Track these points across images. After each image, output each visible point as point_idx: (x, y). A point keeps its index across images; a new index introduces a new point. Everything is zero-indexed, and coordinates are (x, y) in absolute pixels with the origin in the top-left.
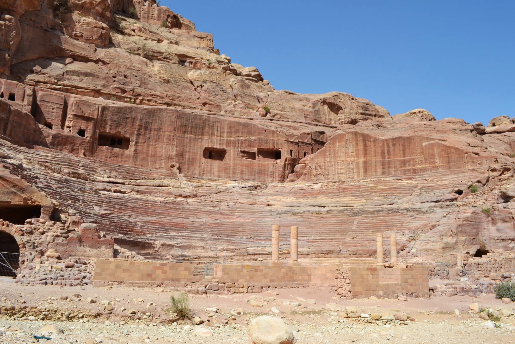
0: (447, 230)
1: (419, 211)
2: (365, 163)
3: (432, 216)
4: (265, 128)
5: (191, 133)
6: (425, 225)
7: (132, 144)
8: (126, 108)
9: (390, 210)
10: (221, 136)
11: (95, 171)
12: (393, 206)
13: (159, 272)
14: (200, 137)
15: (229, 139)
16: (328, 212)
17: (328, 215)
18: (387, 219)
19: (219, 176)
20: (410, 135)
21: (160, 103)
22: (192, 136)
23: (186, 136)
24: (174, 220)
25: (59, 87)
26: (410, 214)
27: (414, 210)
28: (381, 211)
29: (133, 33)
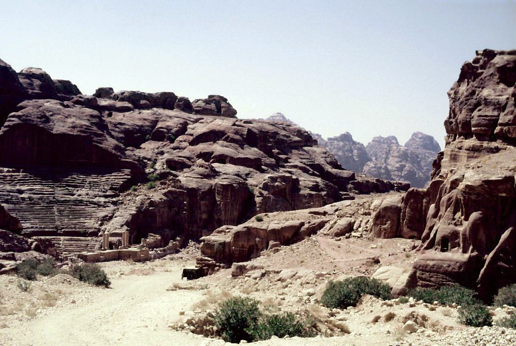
0: (125, 221)
1: (99, 205)
3: (109, 209)
6: (107, 216)
9: (77, 201)
12: (75, 196)
16: (30, 199)
18: (78, 208)
20: (75, 134)
26: (92, 205)
27: (95, 204)
28: (69, 201)
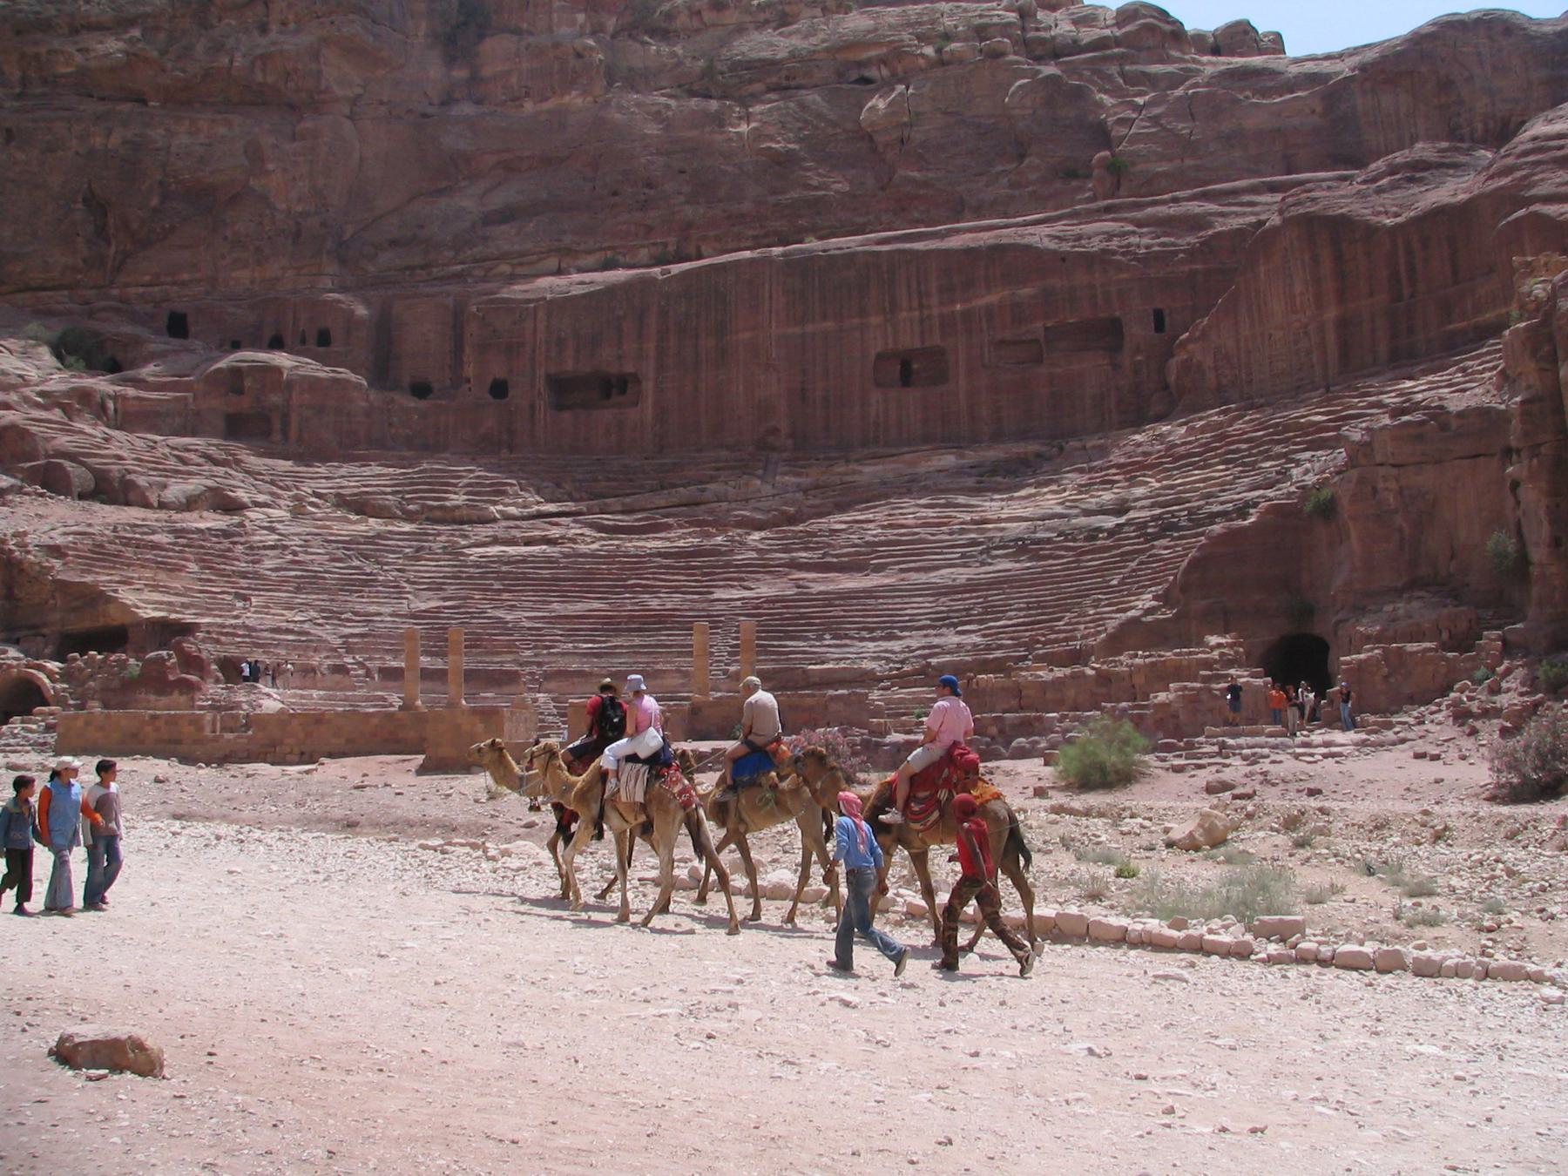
2: (1343, 324)
4: (1066, 247)
5: (825, 317)
7: (649, 386)
8: (611, 290)
10: (921, 306)
11: (504, 493)
13: (149, 729)
14: (856, 321)
15: (945, 310)
17: (1108, 542)
19: (926, 439)
21: (755, 237)
22: (830, 325)
23: (809, 328)
24: (654, 603)
25: (459, 267)
29: (696, 24)
